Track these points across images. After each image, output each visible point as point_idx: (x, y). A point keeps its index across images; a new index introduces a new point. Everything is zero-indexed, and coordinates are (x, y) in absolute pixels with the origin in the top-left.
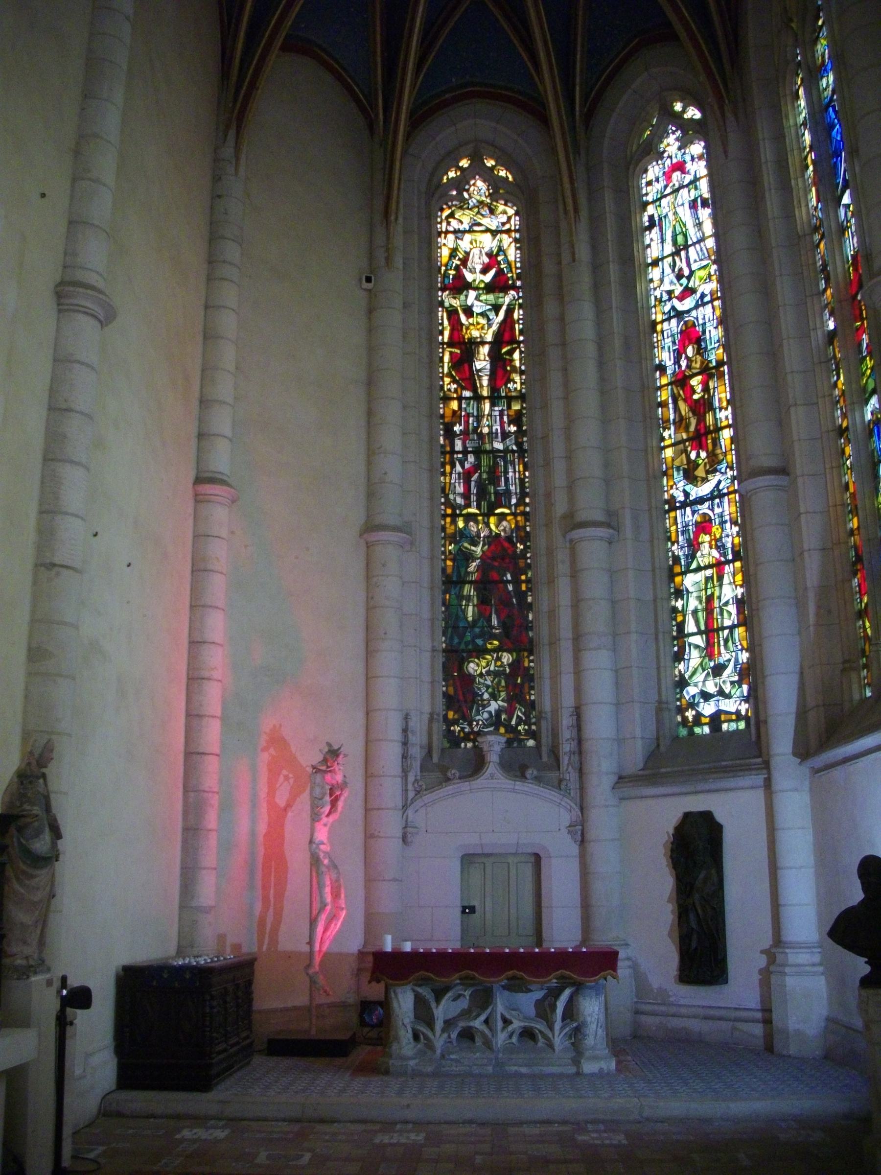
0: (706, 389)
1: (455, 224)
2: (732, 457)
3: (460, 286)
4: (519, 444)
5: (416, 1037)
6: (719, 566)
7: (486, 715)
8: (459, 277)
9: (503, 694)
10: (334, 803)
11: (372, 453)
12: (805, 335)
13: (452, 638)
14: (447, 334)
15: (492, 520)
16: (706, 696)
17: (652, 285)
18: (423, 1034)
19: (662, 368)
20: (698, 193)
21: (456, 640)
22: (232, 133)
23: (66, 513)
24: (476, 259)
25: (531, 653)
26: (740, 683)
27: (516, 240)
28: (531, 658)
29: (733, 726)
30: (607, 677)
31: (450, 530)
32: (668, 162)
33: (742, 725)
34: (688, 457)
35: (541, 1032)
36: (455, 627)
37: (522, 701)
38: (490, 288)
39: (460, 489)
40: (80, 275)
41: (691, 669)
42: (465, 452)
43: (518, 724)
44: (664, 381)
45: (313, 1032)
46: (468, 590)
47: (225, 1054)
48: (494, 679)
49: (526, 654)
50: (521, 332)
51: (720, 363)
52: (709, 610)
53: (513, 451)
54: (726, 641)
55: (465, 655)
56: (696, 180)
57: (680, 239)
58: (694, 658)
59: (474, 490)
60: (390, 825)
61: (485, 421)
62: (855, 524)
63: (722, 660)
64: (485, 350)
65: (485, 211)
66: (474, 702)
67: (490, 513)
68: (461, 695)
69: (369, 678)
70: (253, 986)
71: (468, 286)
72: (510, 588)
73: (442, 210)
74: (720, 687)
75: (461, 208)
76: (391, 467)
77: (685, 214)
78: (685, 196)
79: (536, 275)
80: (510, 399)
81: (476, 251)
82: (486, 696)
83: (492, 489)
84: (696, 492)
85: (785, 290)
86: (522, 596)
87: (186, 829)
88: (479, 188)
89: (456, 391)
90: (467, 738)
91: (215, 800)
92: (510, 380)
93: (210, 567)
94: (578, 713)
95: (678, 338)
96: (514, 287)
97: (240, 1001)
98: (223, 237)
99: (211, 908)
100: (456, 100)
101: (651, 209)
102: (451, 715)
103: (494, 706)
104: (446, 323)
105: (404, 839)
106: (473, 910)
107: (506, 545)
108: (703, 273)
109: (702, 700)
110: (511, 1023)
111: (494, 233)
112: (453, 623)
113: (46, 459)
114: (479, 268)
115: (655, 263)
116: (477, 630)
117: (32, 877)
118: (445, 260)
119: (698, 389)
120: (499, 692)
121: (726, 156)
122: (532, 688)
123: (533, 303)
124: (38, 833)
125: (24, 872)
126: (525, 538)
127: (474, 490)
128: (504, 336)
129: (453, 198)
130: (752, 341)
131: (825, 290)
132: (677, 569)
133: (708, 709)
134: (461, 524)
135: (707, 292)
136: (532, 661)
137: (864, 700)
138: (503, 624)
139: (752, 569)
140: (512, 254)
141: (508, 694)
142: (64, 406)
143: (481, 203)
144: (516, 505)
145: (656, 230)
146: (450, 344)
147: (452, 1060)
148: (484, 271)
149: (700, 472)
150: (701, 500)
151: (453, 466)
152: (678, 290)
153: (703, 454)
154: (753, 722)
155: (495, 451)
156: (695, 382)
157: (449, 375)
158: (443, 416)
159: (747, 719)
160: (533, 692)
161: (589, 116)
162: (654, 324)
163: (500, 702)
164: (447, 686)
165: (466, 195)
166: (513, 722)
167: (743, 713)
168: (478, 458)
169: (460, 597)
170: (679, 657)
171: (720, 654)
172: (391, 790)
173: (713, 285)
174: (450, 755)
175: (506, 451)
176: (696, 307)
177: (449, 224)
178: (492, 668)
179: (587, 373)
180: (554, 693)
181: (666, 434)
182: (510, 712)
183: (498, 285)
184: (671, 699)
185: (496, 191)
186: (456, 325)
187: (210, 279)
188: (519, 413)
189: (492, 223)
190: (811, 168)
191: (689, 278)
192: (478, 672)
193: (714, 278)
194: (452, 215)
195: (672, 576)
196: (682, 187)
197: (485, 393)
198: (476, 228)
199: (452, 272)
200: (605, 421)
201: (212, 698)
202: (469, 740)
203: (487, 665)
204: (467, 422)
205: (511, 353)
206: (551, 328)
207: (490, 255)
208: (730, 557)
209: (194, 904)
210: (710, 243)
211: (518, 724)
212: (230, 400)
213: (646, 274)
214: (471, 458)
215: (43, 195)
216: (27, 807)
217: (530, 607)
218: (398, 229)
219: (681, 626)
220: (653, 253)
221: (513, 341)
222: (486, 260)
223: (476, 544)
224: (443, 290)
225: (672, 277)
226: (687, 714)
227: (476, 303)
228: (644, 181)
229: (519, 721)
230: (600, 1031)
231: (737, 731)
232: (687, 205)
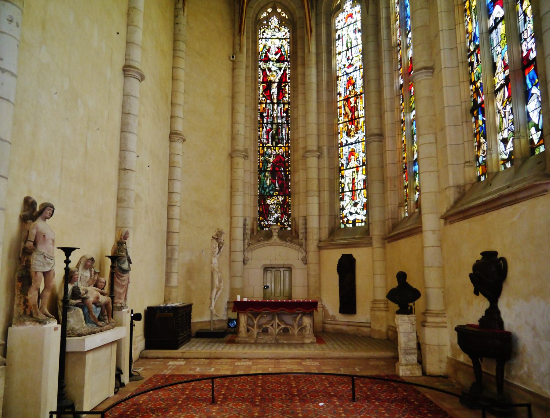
0: (356, 103)
1: (265, 35)
2: (363, 128)
3: (267, 60)
4: (287, 121)
5: (248, 330)
6: (357, 167)
7: (273, 219)
8: (267, 56)
9: (279, 211)
10: (220, 250)
11: (233, 123)
12: (392, 85)
13: (261, 191)
14: (261, 78)
15: (277, 148)
16: (351, 214)
17: (338, 62)
19: (340, 94)
20: (357, 27)
21: (263, 192)
23: (130, 151)
24: (273, 49)
25: (289, 197)
26: (363, 209)
27: (288, 42)
29: (360, 225)
30: (316, 207)
31: (262, 152)
32: (346, 14)
33: (363, 224)
34: (348, 128)
36: (263, 187)
37: (286, 214)
38: (278, 61)
39: (265, 137)
40: (132, 63)
41: (346, 204)
42: (267, 123)
43: (284, 222)
44: (341, 99)
46: (267, 174)
50: (289, 78)
51: (361, 93)
52: (353, 184)
53: (285, 123)
54: (359, 194)
56: (356, 21)
57: (349, 45)
58: (347, 199)
59: (270, 137)
60: (239, 257)
61: (275, 112)
62: (405, 155)
63: (357, 201)
64: (276, 85)
65: (277, 30)
66: (269, 214)
67: (276, 146)
68: (265, 212)
69: (231, 205)
71: (270, 60)
72: (283, 173)
73: (261, 29)
75: (268, 29)
76: (241, 128)
77: (352, 35)
78: (352, 28)
79: (295, 57)
80: (284, 104)
81: (273, 47)
82: (273, 212)
83: (277, 137)
84: (350, 140)
85: (386, 68)
86: (287, 176)
88: (274, 21)
89: (264, 100)
90: (266, 227)
92: (284, 97)
93: (175, 165)
94: (305, 219)
95: (346, 83)
96: (287, 61)
98: (179, 40)
99: (177, 286)
101: (339, 32)
102: (261, 218)
103: (276, 216)
104: (261, 74)
105: (244, 262)
106: (268, 287)
107: (282, 158)
108: (357, 58)
111: (280, 39)
112: (262, 186)
113: (122, 131)
114: (274, 53)
115: (339, 53)
116: (271, 188)
117: (122, 277)
118: (261, 49)
119: (353, 102)
122: (290, 209)
123: (293, 68)
124: (124, 263)
125: (120, 275)
126: (288, 155)
127: (270, 137)
128: (282, 80)
129: (265, 25)
130: (373, 86)
131: (400, 69)
132: (342, 168)
133: (351, 218)
134: (265, 150)
135: (358, 66)
137: (405, 217)
138: (279, 186)
139: (369, 170)
140: (287, 48)
142: (127, 112)
143: (276, 27)
144: (286, 143)
145: (340, 40)
146: (263, 82)
148: (276, 54)
149: (352, 133)
150: (352, 144)
151: (263, 128)
152: (347, 64)
153: (353, 127)
154: (367, 223)
155: (278, 123)
156: (352, 100)
157: (262, 94)
158: (259, 110)
159: (365, 222)
162: (338, 77)
165: (270, 23)
167: (364, 220)
168: (272, 126)
169: (265, 176)
170: (342, 199)
172: (239, 245)
173: (360, 63)
175: (282, 123)
176: (354, 71)
177: (263, 35)
179: (313, 95)
181: (340, 119)
183: (281, 60)
185: (281, 22)
186: (265, 75)
187: (174, 57)
188: (287, 109)
189: (280, 35)
190: (399, 21)
191: (351, 60)
193: (361, 60)
194: (264, 32)
195: (340, 170)
196: (350, 24)
197: (275, 101)
198: (273, 37)
199: (264, 54)
200: (319, 113)
201: (176, 213)
204: (268, 112)
205: (285, 86)
206: (300, 78)
207: (278, 48)
208: (361, 164)
209: (170, 285)
210: (360, 47)
211: (284, 222)
212: (183, 104)
213: (336, 58)
214: (270, 126)
215: (118, 33)
216: (120, 253)
217: (290, 180)
218: (244, 38)
219: (343, 188)
220: (338, 50)
221: (286, 82)
222: (277, 50)
223: (270, 157)
224: (261, 61)
225: (346, 59)
227: (273, 67)
228: (337, 21)
230: (311, 329)
231: (362, 226)
232: (352, 31)
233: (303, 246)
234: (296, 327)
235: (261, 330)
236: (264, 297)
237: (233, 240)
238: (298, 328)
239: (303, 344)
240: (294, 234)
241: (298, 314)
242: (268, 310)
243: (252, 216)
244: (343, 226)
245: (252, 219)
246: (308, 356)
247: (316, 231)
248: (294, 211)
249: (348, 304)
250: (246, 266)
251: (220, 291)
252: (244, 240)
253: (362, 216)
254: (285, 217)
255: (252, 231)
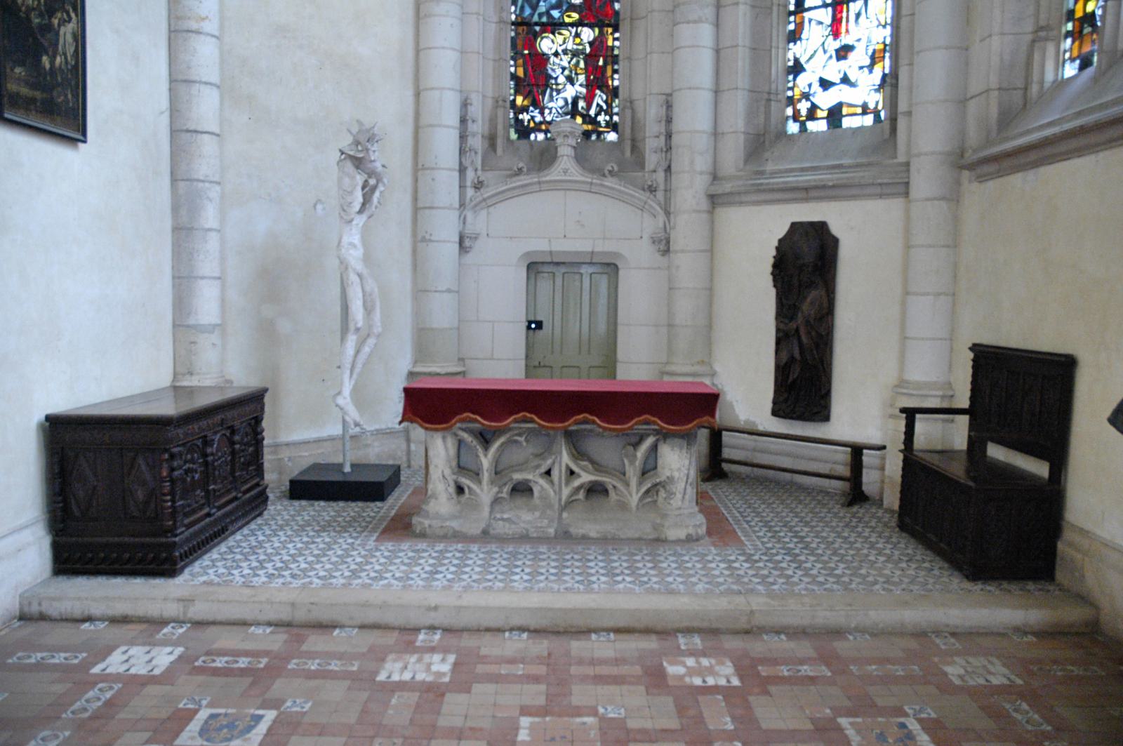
5: (460, 490)
7: (561, 103)
9: (582, 78)
13: (522, 8)
16: (825, 84)
18: (469, 487)
21: (528, 11)
25: (616, 29)
28: (617, 35)
30: (706, 60)
33: (869, 120)
35: (614, 487)
43: (598, 114)
45: (347, 469)
47: (208, 520)
48: (572, 59)
49: (610, 30)
54: (858, 15)
55: (537, 28)
60: (445, 227)
66: (547, 86)
69: (418, 51)
70: (264, 424)
74: (845, 74)
82: (562, 79)
87: (176, 229)
90: (537, 129)
91: (214, 192)
97: (237, 446)
102: (519, 100)
103: (570, 92)
106: (539, 325)
109: (820, 89)
110: (579, 476)
120: (577, 74)
122: (615, 71)
133: (825, 100)
136: (615, 39)
141: (587, 79)
147: (502, 519)
160: (616, 76)
163: (577, 87)
164: (516, 66)
166: (592, 112)
167: (871, 106)
170: (794, 37)
171: (847, 31)
172: (445, 186)
174: (513, 141)
178: (570, 47)
180: (638, 78)
182: (589, 99)
184: (780, 88)
192: (553, 51)
201: (205, 57)
202: (540, 131)
203: (564, 43)
209: (192, 321)
211: (598, 114)
226: (799, 106)
229: (600, 110)
231: (861, 128)
233: (660, 194)
234: (634, 482)
235: (507, 489)
236: (527, 357)
237: (424, 168)
238: (640, 484)
239: (660, 541)
240: (628, 153)
241: (641, 439)
242: (532, 421)
243: (490, 94)
244: (793, 128)
245: (490, 102)
246: (685, 624)
247: (703, 142)
248: (629, 78)
249: (804, 383)
250: (469, 258)
251: (371, 341)
252: (462, 170)
253: (865, 90)
254: (600, 98)
255: (491, 140)
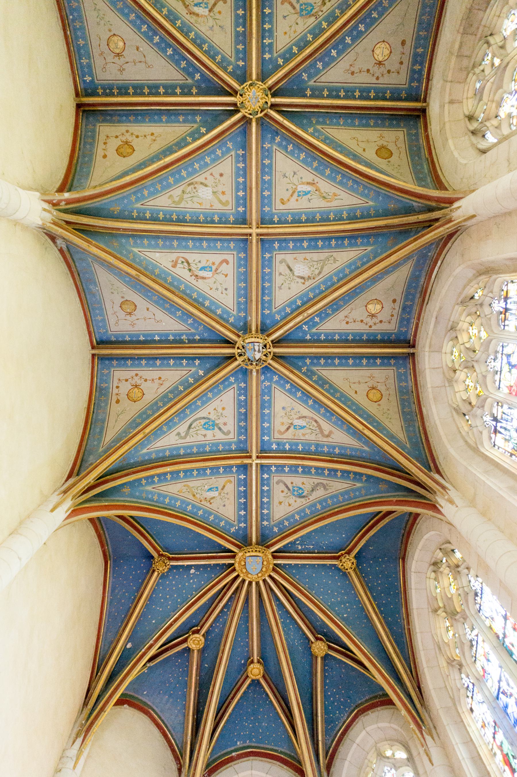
22: (79, 740)
100: (239, 757)
121: (433, 765)
161: (329, 767)
